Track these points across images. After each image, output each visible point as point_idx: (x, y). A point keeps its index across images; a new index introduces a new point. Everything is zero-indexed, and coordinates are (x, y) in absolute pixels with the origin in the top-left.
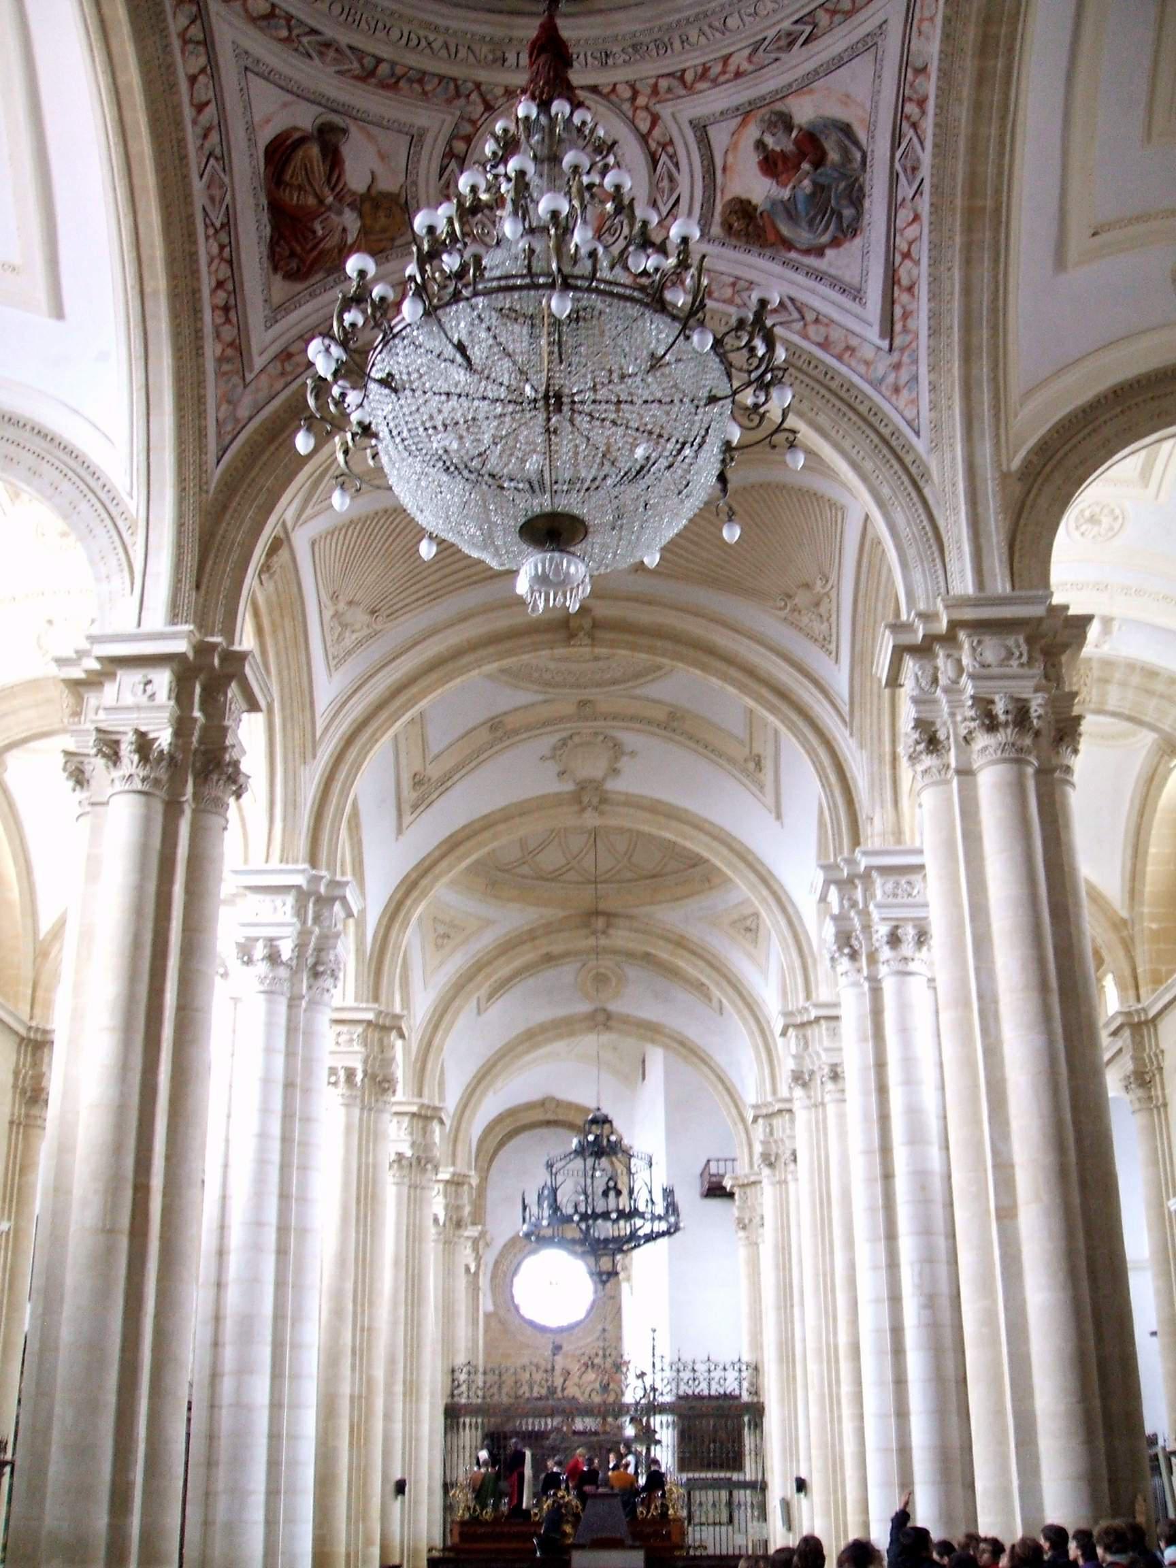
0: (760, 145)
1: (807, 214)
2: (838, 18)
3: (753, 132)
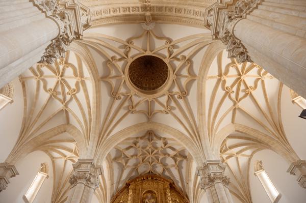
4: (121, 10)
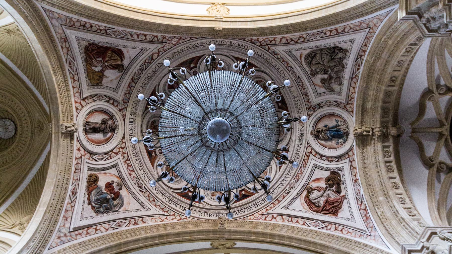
0: (113, 182)
1: (100, 198)
2: (147, 197)
3: (116, 180)
4: (391, 175)
